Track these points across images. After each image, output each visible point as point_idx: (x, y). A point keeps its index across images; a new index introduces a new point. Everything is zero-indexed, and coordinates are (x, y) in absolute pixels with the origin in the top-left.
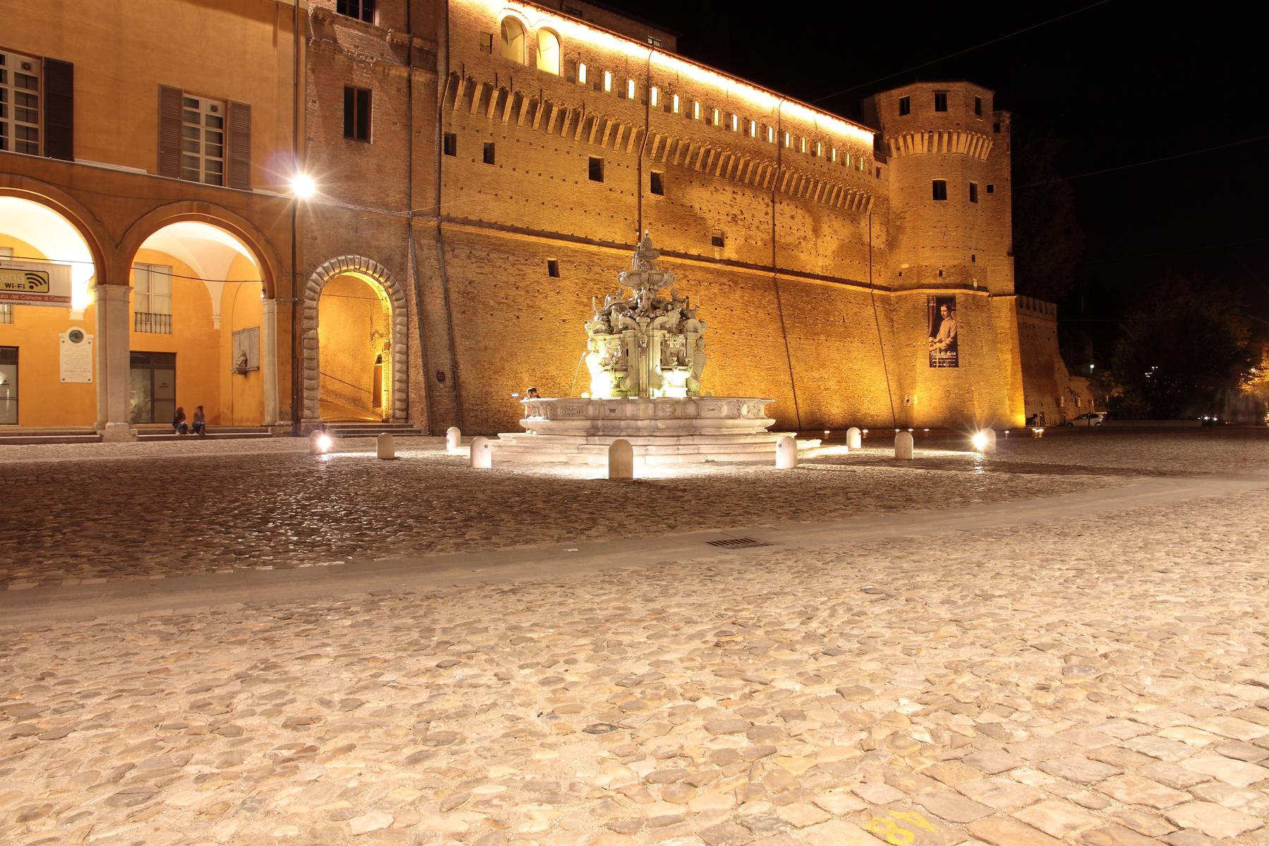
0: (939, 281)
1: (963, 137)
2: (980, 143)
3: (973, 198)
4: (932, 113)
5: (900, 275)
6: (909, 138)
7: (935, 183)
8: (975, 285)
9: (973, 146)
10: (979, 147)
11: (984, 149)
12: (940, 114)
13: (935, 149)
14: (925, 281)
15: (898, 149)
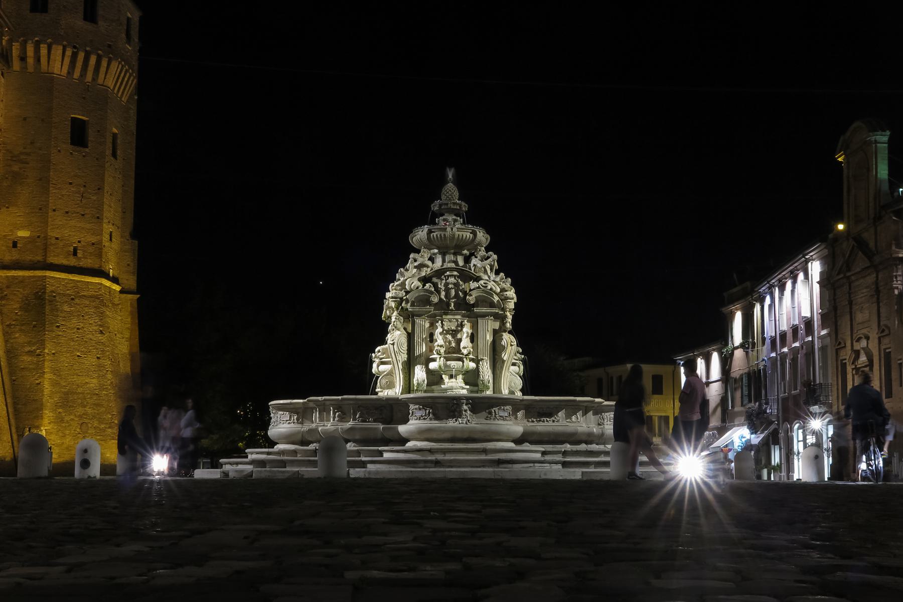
0: (72, 262)
1: (114, 65)
2: (126, 79)
3: (114, 155)
4: (79, 22)
5: (15, 245)
6: (44, 51)
7: (74, 120)
8: (111, 275)
9: (119, 84)
10: (124, 83)
11: (128, 87)
12: (88, 26)
13: (77, 74)
14: (52, 260)
15: (23, 59)
